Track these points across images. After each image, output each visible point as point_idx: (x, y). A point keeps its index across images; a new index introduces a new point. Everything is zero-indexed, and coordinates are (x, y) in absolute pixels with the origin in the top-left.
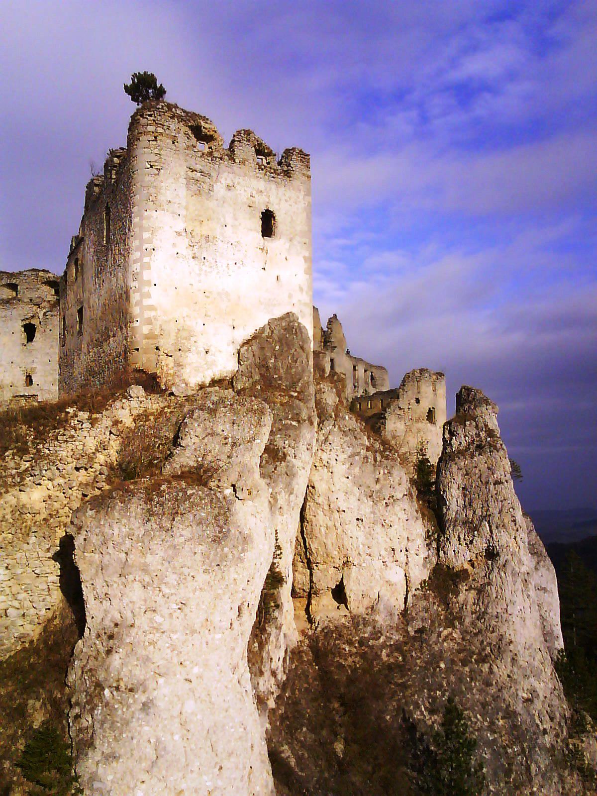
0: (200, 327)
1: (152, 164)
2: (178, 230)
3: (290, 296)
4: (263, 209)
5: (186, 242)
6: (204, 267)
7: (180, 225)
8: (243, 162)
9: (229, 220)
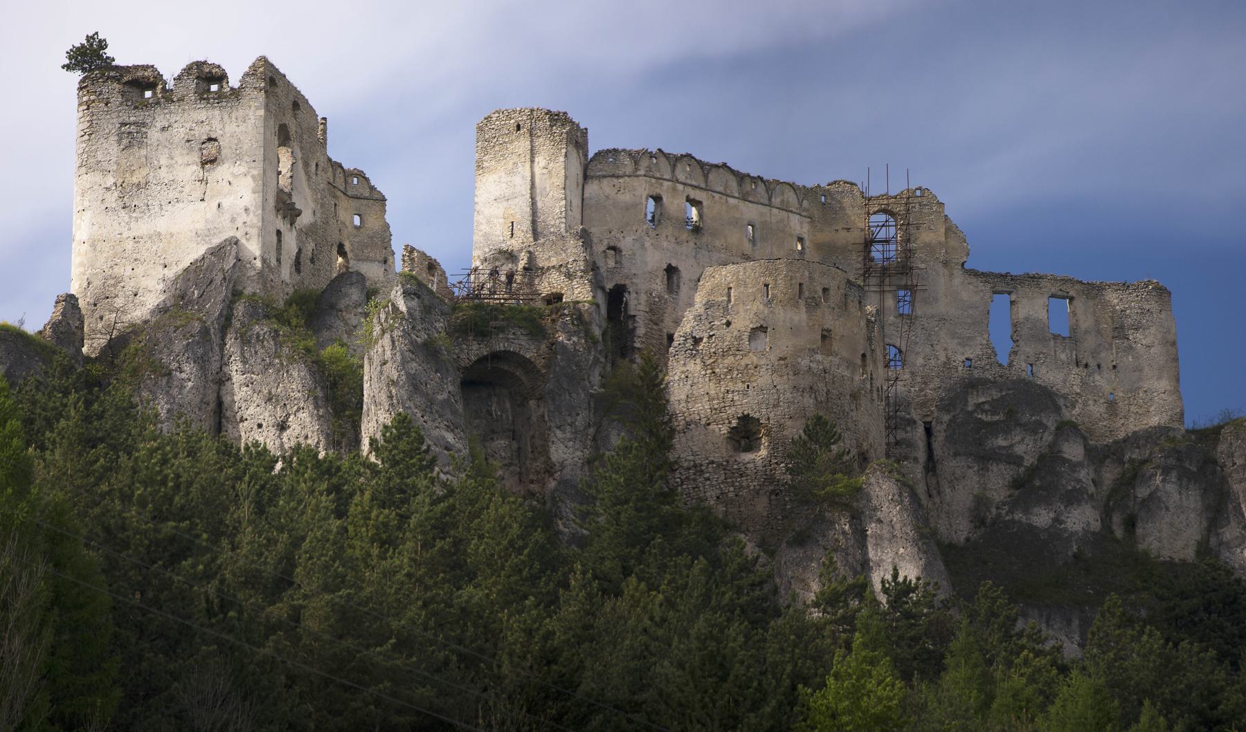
0: (129, 272)
3: (233, 220)
6: (134, 215)
7: (110, 181)
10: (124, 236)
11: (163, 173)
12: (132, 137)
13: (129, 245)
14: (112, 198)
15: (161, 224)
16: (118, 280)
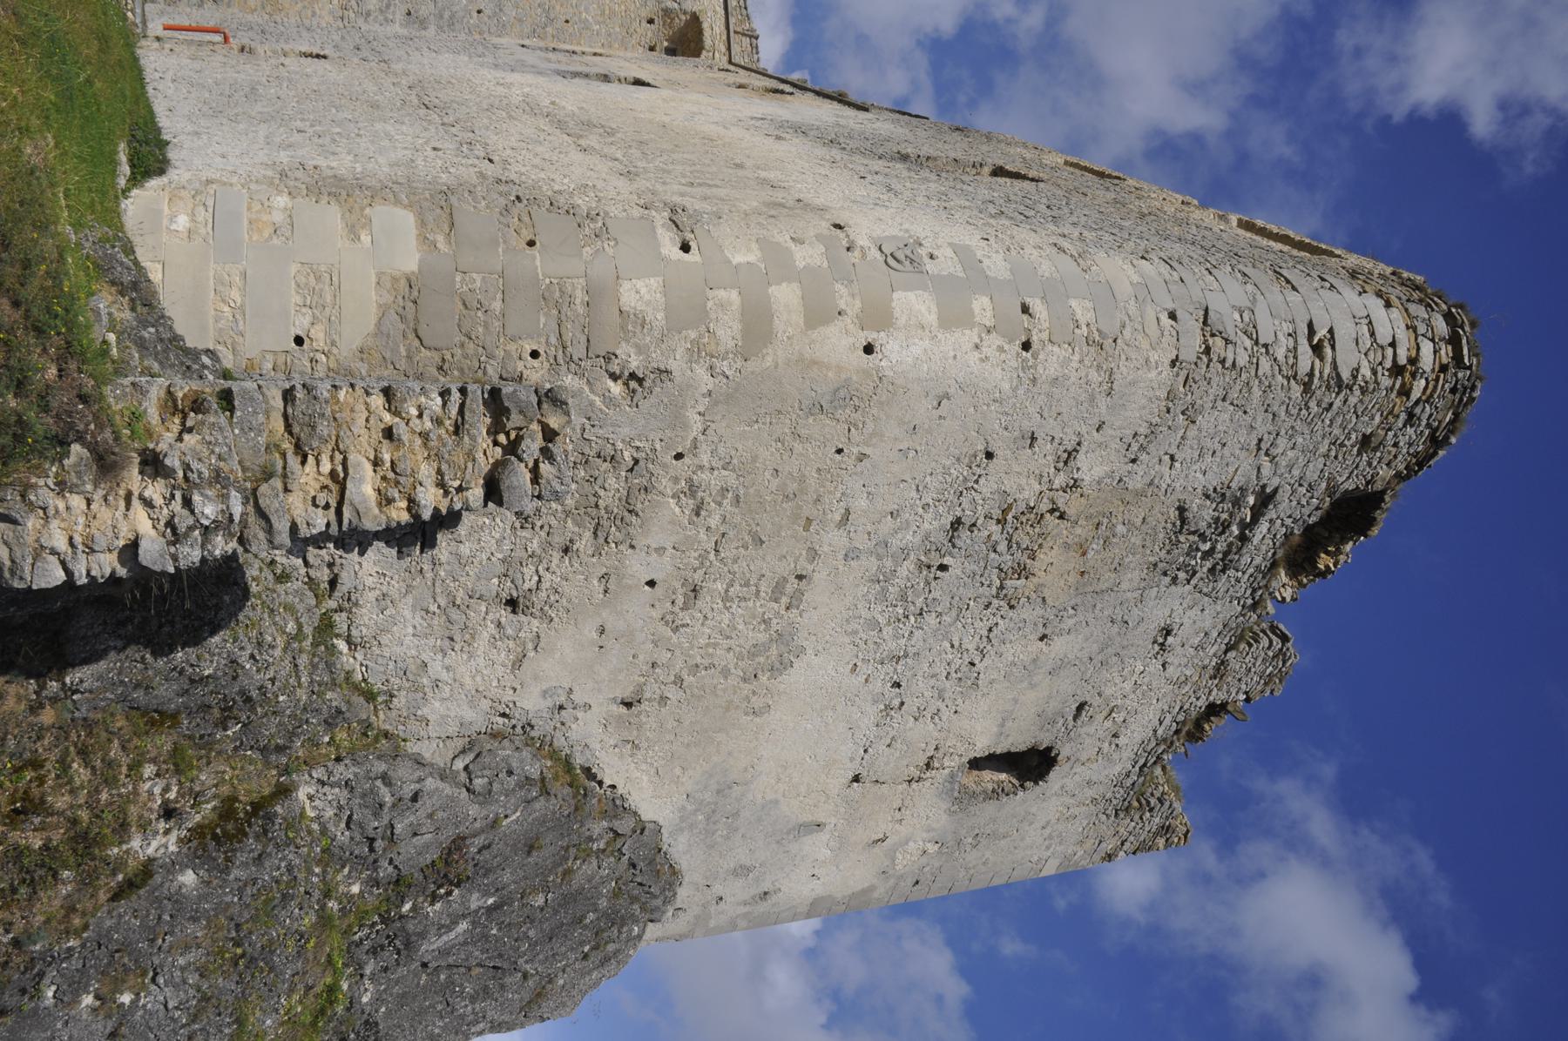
1: (1328, 351)
2: (1082, 460)
3: (742, 871)
4: (1065, 751)
5: (1027, 491)
7: (1090, 468)
8: (1220, 670)
9: (1060, 646)
10: (833, 540)
11: (1020, 648)
12: (1203, 542)
13: (772, 564)
14: (1020, 478)
15: (820, 669)
16: (613, 524)
